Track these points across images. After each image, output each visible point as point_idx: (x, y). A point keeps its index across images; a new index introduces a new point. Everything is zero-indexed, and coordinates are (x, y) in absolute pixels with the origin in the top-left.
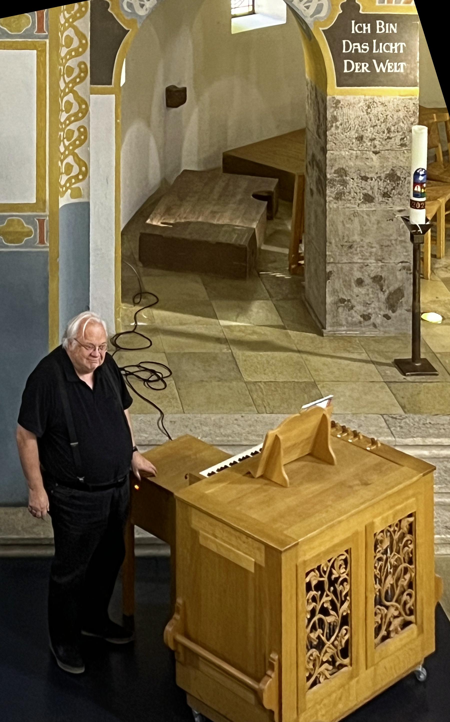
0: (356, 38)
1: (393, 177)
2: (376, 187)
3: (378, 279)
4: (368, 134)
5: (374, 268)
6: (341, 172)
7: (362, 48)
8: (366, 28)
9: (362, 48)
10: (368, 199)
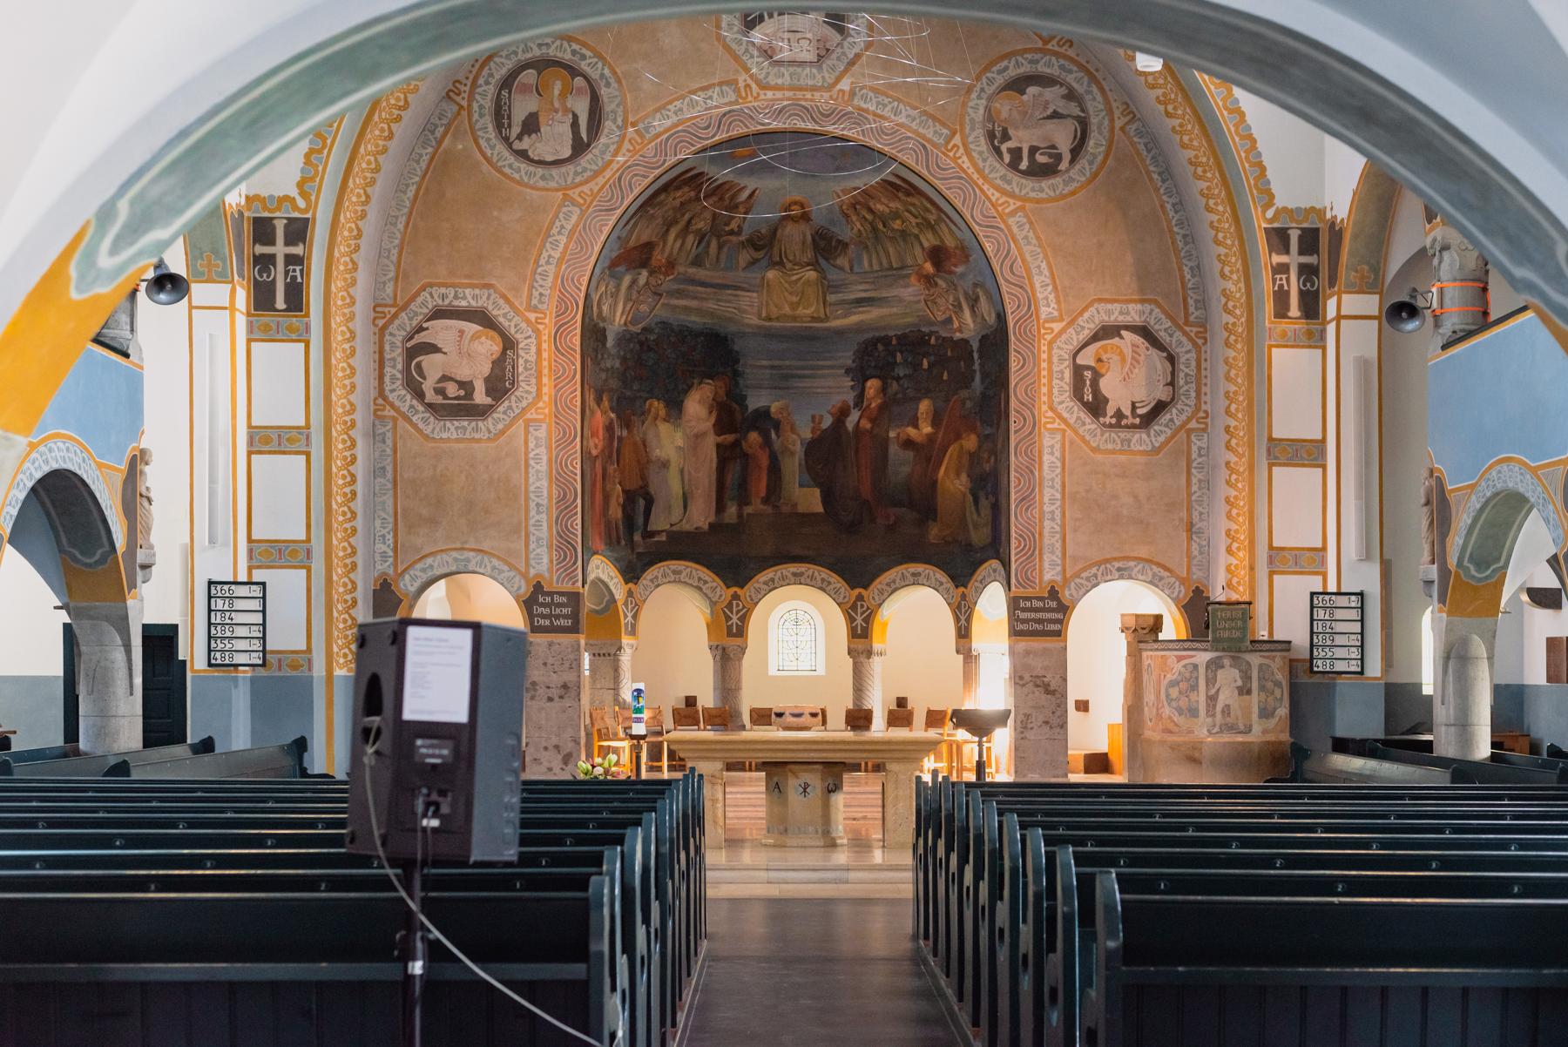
0: (542, 605)
1: (565, 686)
2: (554, 693)
3: (557, 747)
4: (550, 661)
5: (554, 740)
6: (534, 684)
7: (546, 611)
8: (548, 599)
9: (546, 611)
10: (550, 699)
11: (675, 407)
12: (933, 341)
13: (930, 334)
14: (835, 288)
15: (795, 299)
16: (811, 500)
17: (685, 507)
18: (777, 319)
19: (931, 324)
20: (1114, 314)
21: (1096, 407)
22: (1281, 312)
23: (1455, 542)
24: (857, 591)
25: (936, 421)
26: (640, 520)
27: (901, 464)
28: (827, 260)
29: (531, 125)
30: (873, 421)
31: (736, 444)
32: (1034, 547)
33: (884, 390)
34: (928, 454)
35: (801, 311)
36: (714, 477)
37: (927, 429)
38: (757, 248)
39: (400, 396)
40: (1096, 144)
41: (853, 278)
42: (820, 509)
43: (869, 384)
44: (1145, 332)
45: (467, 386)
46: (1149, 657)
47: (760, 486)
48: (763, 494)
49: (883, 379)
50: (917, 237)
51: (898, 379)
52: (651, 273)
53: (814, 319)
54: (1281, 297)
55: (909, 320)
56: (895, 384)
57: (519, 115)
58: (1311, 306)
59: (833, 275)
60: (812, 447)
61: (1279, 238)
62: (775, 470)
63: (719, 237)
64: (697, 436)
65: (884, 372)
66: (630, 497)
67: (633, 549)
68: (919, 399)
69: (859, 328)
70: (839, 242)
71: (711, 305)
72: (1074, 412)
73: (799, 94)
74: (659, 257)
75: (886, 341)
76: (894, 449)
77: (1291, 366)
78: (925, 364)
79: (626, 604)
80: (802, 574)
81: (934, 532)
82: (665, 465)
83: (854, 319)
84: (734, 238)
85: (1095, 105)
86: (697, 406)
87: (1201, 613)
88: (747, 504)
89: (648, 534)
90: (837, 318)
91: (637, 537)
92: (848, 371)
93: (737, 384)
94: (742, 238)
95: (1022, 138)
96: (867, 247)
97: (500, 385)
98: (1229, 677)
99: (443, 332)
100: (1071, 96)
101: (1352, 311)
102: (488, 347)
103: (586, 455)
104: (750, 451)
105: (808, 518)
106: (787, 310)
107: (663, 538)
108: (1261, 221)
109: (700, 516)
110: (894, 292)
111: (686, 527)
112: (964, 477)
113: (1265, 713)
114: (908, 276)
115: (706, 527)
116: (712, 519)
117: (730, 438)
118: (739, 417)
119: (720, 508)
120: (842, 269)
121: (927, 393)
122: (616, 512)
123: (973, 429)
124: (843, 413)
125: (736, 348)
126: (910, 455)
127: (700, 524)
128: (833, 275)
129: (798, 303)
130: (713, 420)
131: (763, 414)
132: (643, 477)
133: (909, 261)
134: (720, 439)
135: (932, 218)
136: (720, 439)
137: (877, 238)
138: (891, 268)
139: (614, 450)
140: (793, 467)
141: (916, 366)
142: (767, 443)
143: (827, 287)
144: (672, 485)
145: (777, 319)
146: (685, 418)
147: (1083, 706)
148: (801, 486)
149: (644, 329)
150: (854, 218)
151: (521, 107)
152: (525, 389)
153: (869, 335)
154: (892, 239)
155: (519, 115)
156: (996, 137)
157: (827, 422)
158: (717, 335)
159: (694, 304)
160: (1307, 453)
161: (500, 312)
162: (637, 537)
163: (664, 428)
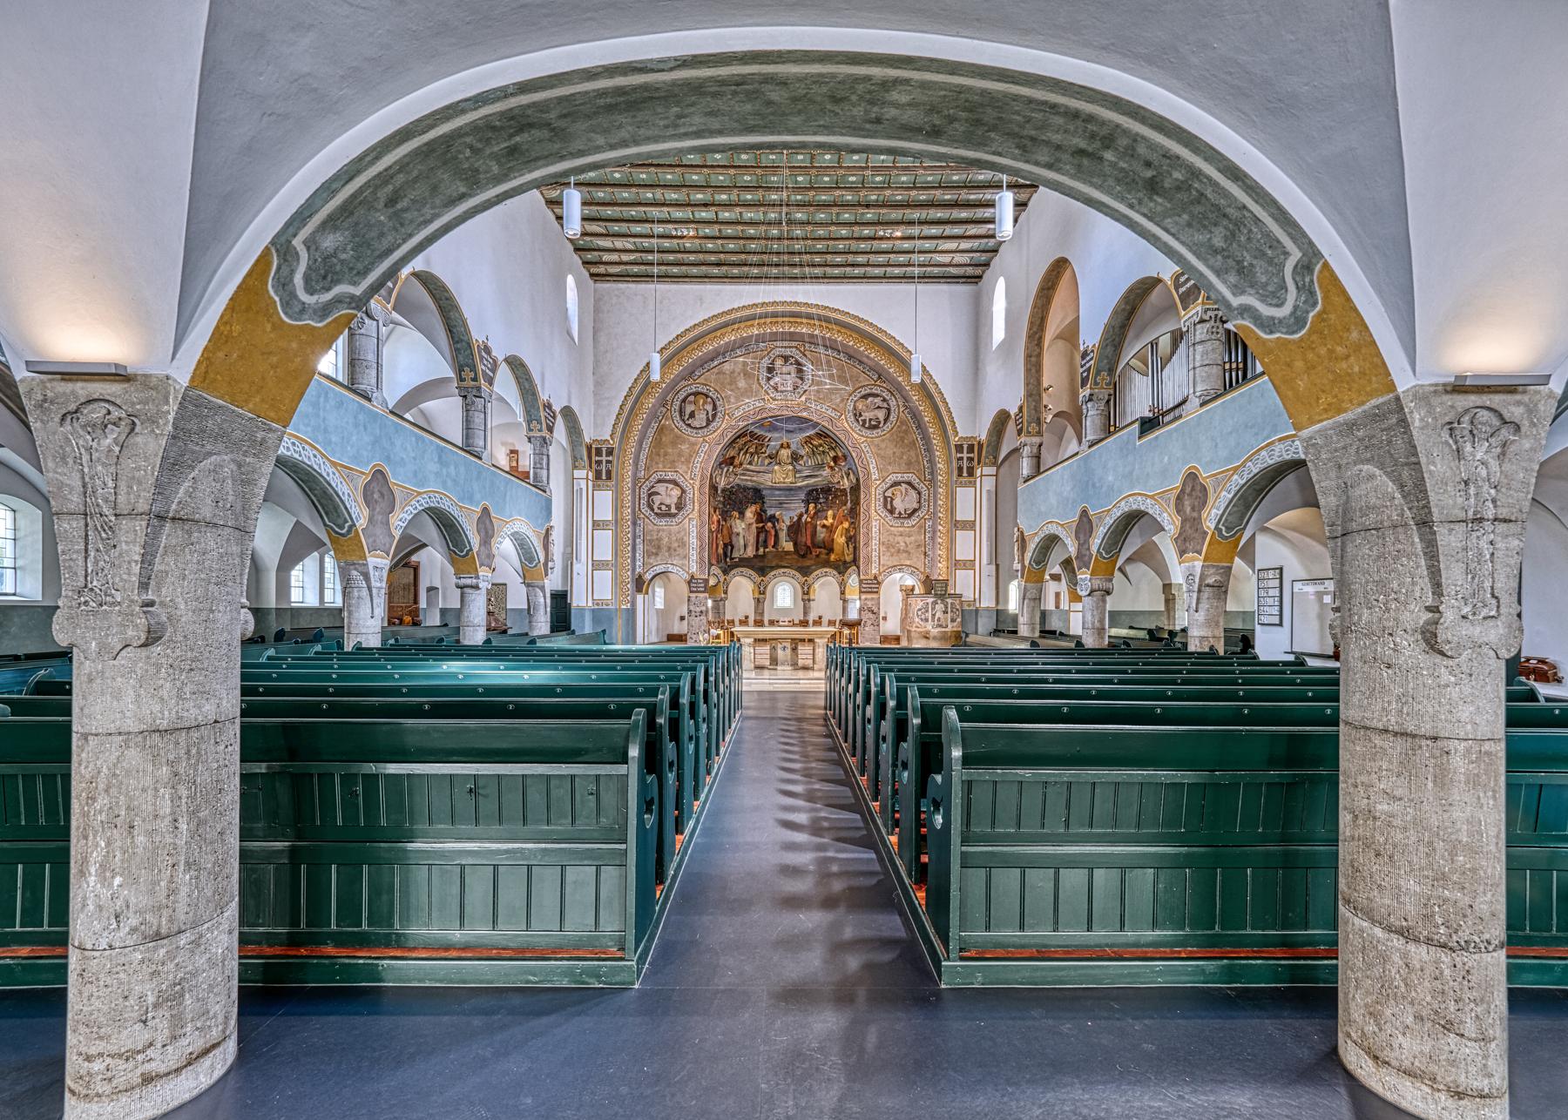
11: (742, 514)
14: (797, 471)
20: (899, 477)
21: (892, 512)
22: (960, 475)
23: (1028, 555)
27: (822, 534)
29: (692, 415)
32: (869, 560)
34: (830, 529)
39: (645, 509)
40: (893, 418)
44: (909, 484)
45: (668, 506)
46: (911, 600)
54: (960, 469)
57: (688, 411)
58: (971, 473)
60: (789, 528)
61: (959, 448)
62: (776, 536)
66: (726, 545)
72: (884, 513)
74: (737, 462)
77: (965, 496)
81: (833, 557)
85: (893, 403)
86: (750, 514)
87: (929, 585)
95: (867, 415)
97: (680, 507)
98: (940, 607)
99: (661, 488)
100: (884, 400)
101: (986, 477)
102: (676, 492)
103: (710, 531)
105: (788, 553)
108: (954, 440)
109: (750, 552)
113: (953, 620)
122: (721, 551)
124: (801, 516)
131: (773, 516)
139: (720, 530)
140: (783, 535)
147: (885, 618)
151: (689, 408)
152: (689, 507)
155: (688, 411)
156: (857, 415)
160: (969, 526)
161: (680, 480)
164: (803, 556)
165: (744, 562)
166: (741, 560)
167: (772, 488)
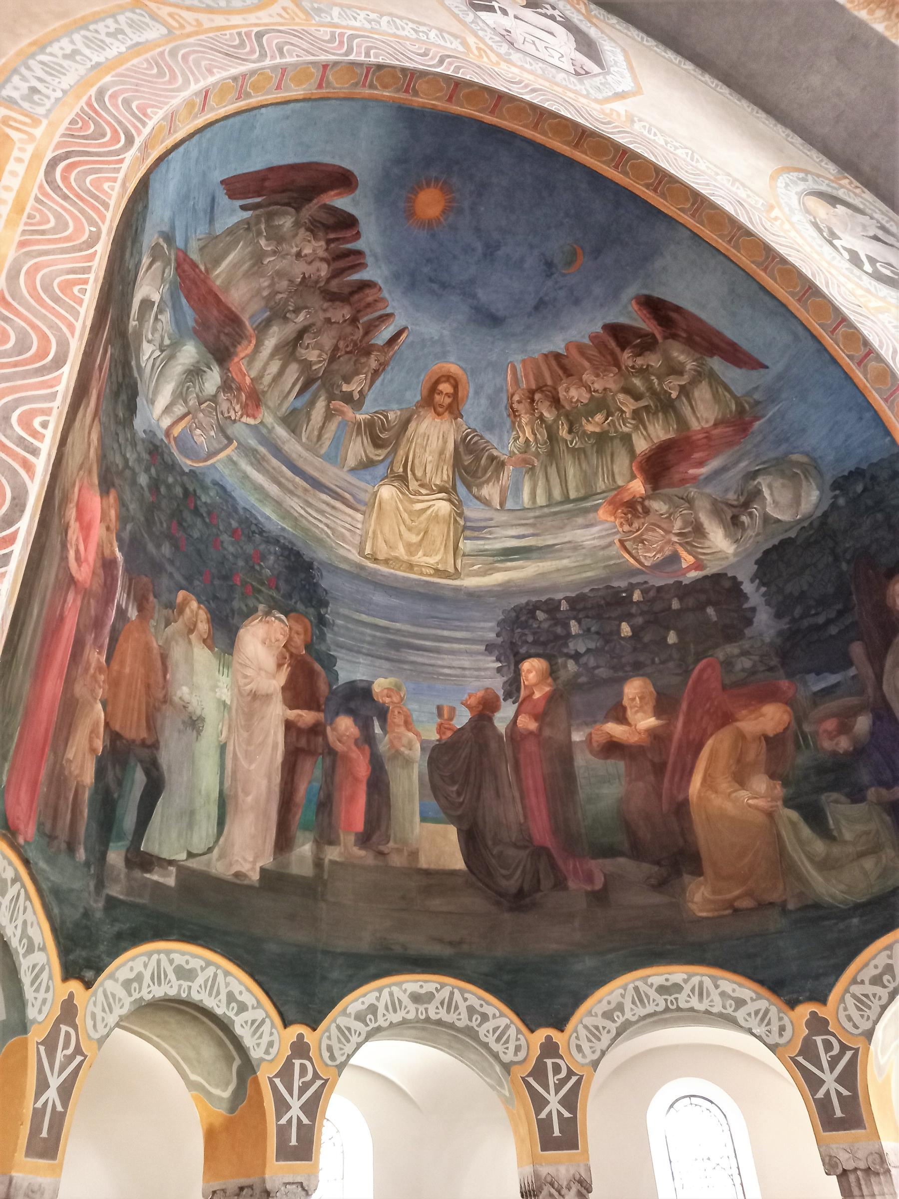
11: (224, 633)
12: (637, 596)
13: (631, 588)
15: (414, 539)
16: (441, 846)
17: (221, 823)
18: (386, 562)
19: (634, 573)
24: (542, 1034)
25: (664, 705)
26: (129, 820)
28: (469, 487)
30: (536, 717)
31: (316, 730)
33: (553, 673)
35: (420, 558)
36: (277, 779)
37: (646, 722)
38: (377, 443)
41: (503, 517)
42: (458, 863)
43: (526, 665)
47: (355, 811)
48: (360, 826)
49: (549, 658)
50: (626, 439)
51: (576, 656)
52: (227, 385)
53: (438, 572)
55: (589, 574)
56: (572, 666)
59: (474, 512)
60: (442, 756)
62: (378, 784)
63: (331, 398)
64: (255, 696)
65: (551, 647)
66: (118, 753)
67: (100, 885)
68: (620, 681)
69: (505, 591)
70: (492, 458)
71: (294, 504)
73: (556, 88)
75: (551, 607)
76: (582, 760)
78: (626, 629)
79: (50, 1043)
80: (430, 997)
81: (700, 897)
82: (195, 723)
83: (498, 578)
84: (349, 412)
88: (331, 843)
89: (142, 861)
90: (468, 575)
91: (115, 857)
92: (490, 648)
93: (322, 637)
94: (361, 417)
96: (533, 469)
104: (339, 747)
106: (401, 552)
107: (171, 881)
110: (568, 536)
111: (219, 868)
112: (760, 784)
114: (596, 508)
115: (255, 876)
116: (267, 860)
117: (307, 717)
118: (323, 688)
119: (284, 841)
120: (487, 503)
121: (637, 669)
122: (84, 770)
123: (770, 695)
124: (485, 709)
125: (324, 584)
126: (618, 766)
127: (245, 868)
128: (474, 512)
129: (420, 544)
130: (282, 678)
132: (151, 724)
133: (601, 485)
134: (292, 714)
135: (672, 386)
136: (292, 714)
137: (552, 455)
138: (567, 500)
140: (409, 784)
141: (609, 636)
142: (368, 739)
143: (464, 527)
144: (195, 772)
145: (386, 562)
146: (238, 658)
148: (424, 819)
149: (193, 473)
150: (525, 419)
153: (523, 600)
154: (576, 453)
157: (462, 718)
158: (298, 554)
159: (273, 490)
162: (115, 857)
163: (202, 656)
164: (520, 901)
165: (201, 911)
166: (197, 886)
167: (359, 575)
